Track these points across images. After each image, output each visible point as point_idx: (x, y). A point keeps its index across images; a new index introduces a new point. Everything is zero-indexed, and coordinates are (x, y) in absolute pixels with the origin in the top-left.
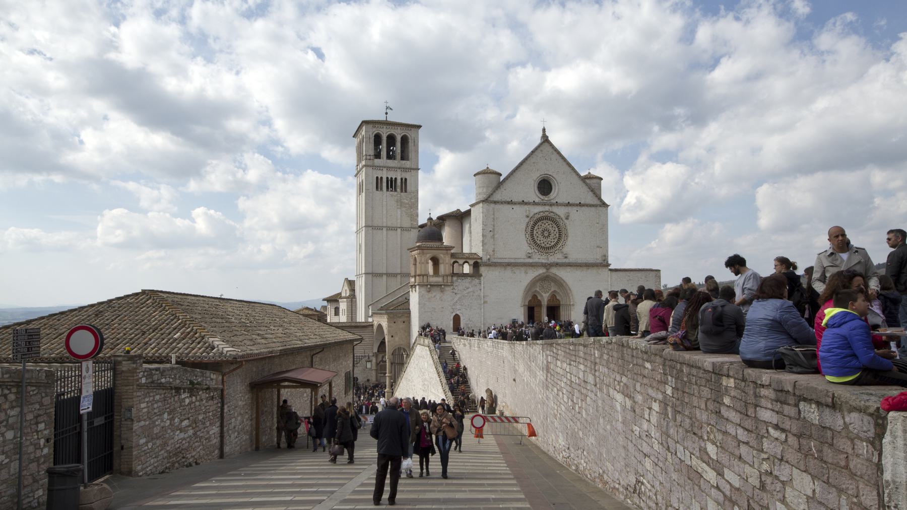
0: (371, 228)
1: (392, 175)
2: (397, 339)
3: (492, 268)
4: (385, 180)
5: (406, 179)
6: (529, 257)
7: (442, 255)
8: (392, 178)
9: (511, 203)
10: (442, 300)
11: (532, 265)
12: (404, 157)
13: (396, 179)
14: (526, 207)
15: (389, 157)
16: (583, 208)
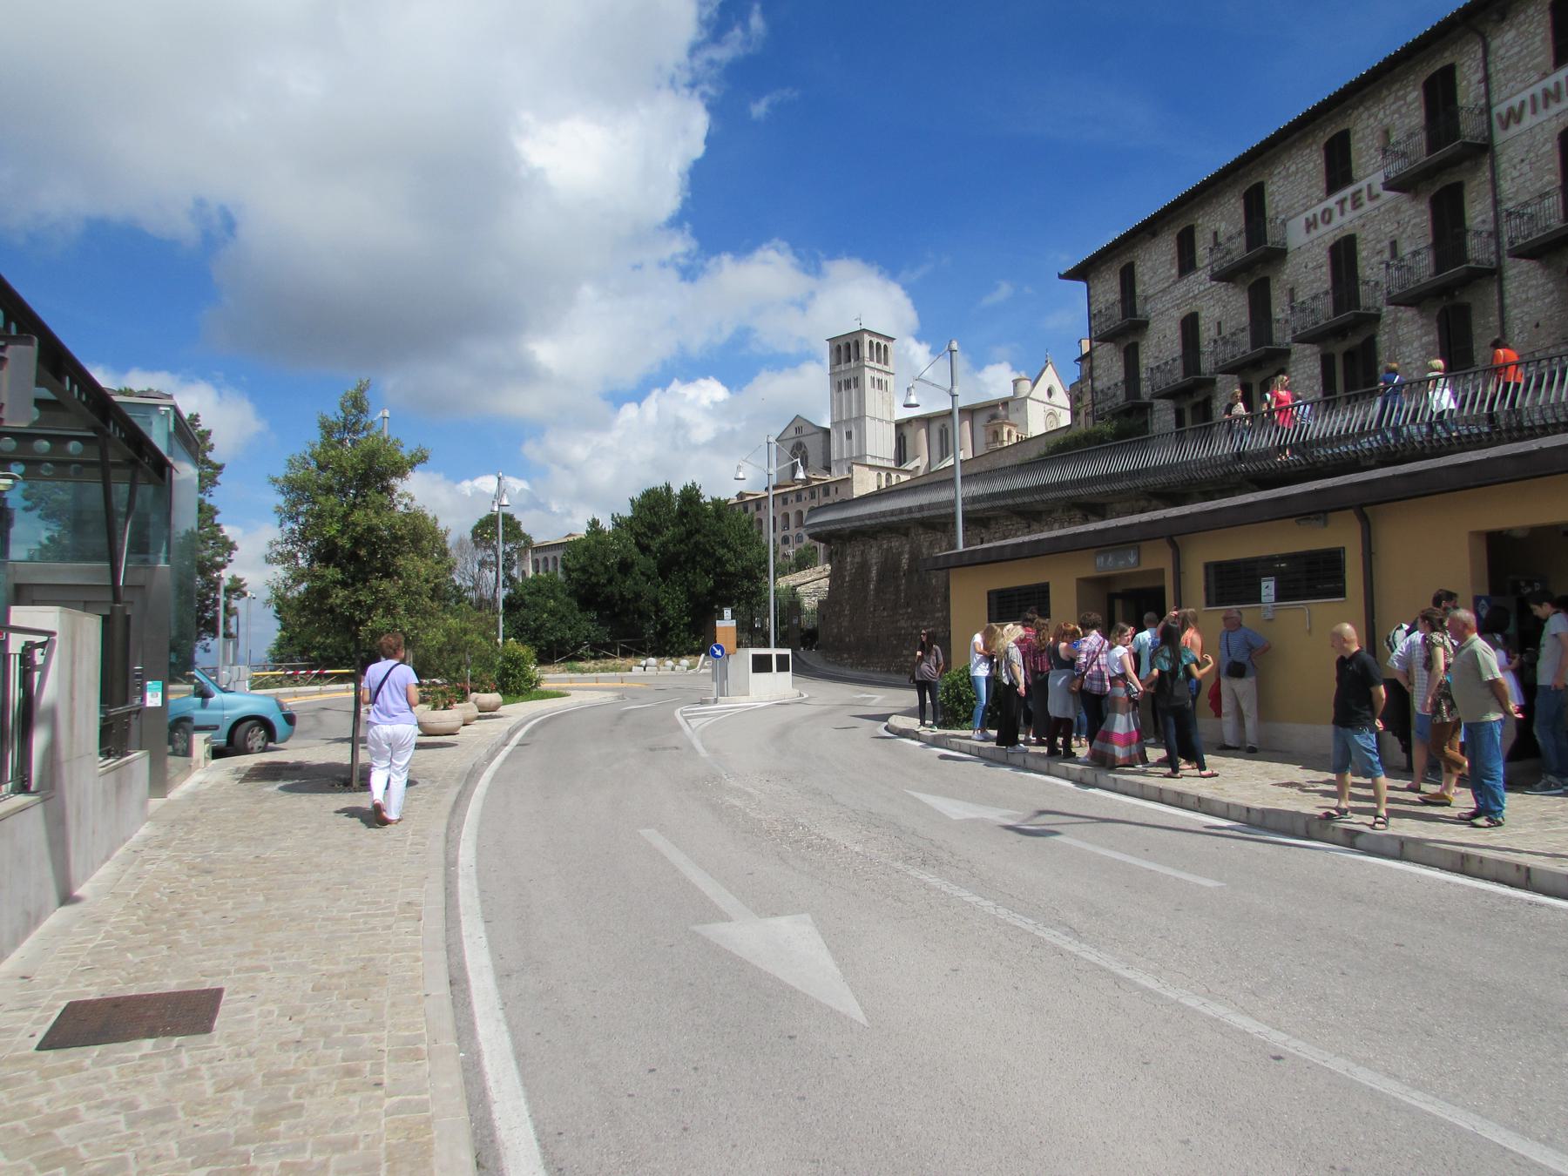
12: (886, 363)
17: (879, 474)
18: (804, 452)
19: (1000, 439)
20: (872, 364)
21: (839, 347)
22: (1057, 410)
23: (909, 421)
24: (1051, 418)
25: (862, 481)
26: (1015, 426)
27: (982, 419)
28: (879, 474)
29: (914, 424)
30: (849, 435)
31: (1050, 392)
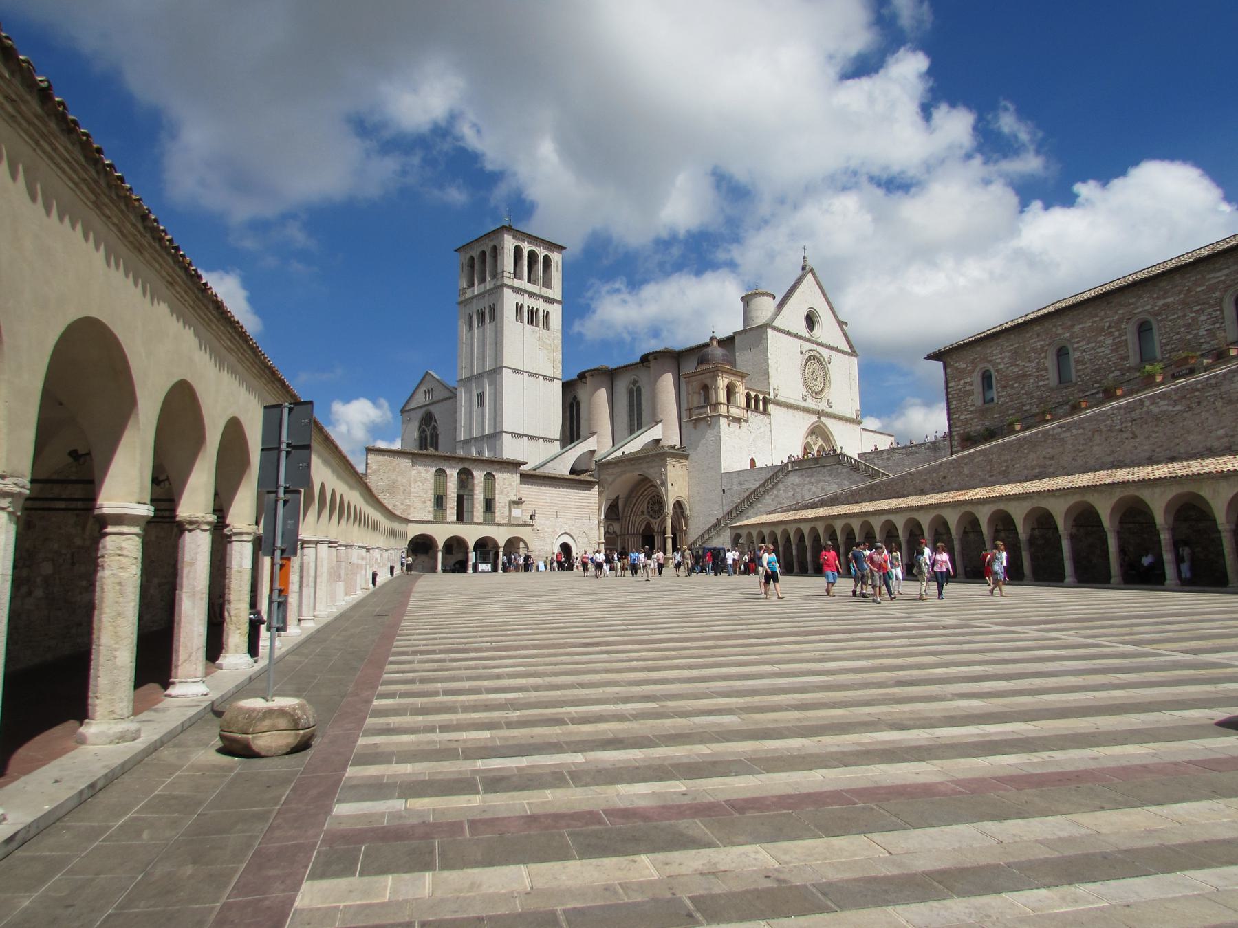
1: (534, 303)
2: (676, 489)
3: (778, 407)
5: (548, 313)
8: (533, 308)
9: (788, 333)
10: (740, 438)
11: (808, 411)
14: (800, 341)
15: (529, 281)
16: (840, 354)
17: (441, 473)
18: (435, 428)
20: (517, 283)
21: (472, 258)
22: (825, 353)
23: (582, 376)
24: (813, 365)
25: (392, 489)
26: (743, 376)
27: (690, 367)
28: (441, 473)
29: (589, 380)
30: (481, 397)
31: (811, 321)
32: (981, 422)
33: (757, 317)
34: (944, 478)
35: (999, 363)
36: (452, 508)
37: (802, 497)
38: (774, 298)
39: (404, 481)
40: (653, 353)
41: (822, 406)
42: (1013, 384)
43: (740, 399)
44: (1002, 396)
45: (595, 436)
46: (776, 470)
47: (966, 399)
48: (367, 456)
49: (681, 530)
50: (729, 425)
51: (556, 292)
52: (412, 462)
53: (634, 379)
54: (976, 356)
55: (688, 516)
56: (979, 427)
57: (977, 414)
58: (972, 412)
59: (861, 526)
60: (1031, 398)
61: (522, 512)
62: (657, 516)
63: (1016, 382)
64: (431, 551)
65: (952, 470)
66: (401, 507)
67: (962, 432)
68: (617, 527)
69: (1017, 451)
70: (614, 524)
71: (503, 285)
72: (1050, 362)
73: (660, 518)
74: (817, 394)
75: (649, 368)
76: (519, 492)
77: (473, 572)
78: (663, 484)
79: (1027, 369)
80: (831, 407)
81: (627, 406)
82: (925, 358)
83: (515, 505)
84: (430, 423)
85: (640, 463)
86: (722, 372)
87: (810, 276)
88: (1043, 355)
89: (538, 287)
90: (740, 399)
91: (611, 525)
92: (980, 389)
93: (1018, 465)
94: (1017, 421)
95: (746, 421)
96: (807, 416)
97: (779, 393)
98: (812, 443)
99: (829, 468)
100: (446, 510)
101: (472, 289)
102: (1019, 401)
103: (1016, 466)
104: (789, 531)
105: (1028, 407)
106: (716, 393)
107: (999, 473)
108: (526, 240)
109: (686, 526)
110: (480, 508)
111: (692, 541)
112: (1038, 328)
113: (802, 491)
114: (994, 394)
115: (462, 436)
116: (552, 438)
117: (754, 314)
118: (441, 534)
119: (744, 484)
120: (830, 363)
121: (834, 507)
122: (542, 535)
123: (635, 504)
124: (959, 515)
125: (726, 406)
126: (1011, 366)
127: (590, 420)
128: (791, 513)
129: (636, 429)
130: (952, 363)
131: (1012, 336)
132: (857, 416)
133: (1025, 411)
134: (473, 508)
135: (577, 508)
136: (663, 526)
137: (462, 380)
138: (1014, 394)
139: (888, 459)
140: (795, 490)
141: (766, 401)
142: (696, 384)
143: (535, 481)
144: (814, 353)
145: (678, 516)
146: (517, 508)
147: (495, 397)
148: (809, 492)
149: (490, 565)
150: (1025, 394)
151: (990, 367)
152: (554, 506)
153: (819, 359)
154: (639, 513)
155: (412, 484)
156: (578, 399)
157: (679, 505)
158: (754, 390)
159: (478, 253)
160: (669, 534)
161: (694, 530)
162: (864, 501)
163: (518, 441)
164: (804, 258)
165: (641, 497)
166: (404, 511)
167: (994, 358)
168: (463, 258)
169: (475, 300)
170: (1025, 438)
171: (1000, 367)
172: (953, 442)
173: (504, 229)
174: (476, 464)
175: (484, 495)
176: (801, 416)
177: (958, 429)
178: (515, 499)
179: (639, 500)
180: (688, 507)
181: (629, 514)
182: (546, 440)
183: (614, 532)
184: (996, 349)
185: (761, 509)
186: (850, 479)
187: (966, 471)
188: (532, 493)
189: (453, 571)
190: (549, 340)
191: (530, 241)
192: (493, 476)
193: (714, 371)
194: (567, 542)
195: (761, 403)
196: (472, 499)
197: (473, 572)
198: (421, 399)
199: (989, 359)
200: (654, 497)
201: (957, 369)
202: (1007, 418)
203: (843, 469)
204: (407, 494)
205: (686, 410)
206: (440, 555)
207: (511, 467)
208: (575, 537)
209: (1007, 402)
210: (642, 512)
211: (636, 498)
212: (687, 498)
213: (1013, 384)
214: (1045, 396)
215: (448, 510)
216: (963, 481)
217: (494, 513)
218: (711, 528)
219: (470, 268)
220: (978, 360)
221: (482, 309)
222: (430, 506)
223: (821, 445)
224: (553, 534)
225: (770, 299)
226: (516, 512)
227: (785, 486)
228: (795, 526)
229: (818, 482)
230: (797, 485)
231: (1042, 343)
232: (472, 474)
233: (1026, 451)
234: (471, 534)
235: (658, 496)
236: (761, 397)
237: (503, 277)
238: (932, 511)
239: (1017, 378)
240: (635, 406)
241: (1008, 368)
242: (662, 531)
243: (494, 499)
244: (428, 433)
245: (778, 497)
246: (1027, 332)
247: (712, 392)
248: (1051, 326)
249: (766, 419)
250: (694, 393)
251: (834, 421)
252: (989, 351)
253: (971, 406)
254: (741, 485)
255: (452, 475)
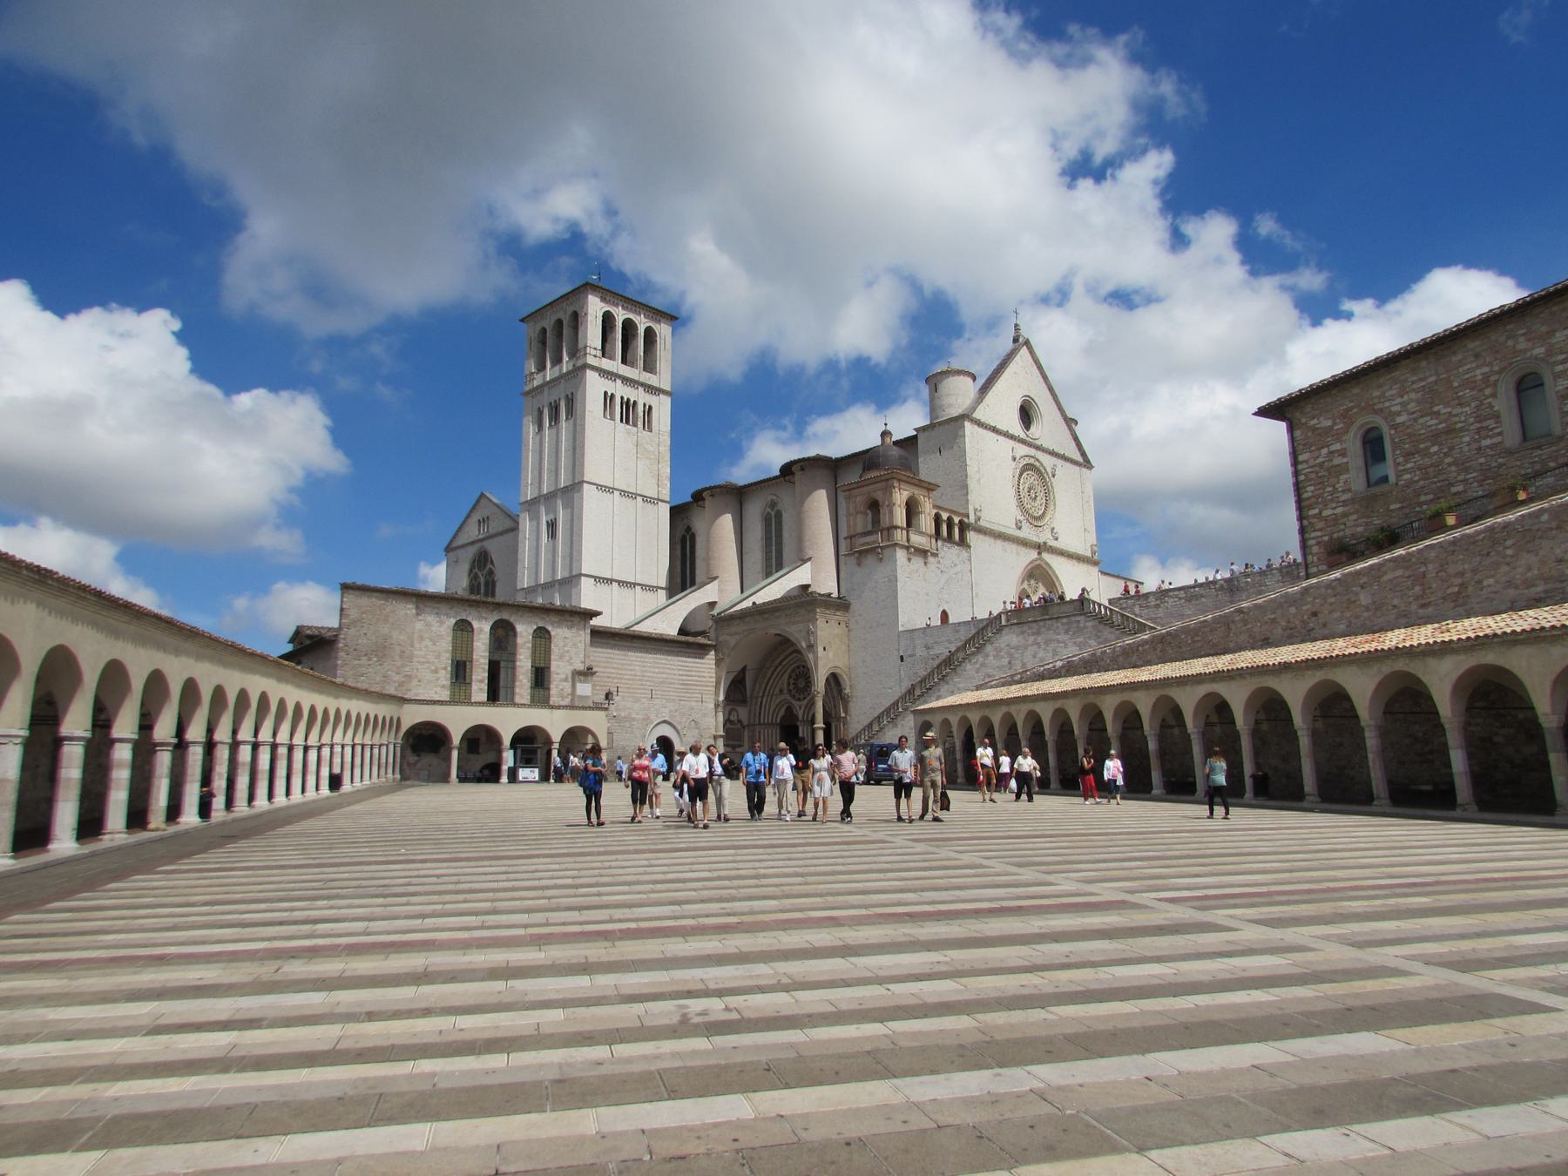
0: (595, 487)
2: (831, 655)
4: (618, 401)
5: (650, 407)
6: (1020, 528)
7: (922, 497)
8: (628, 400)
9: (994, 430)
10: (925, 580)
13: (635, 402)
14: (1011, 443)
15: (622, 362)
16: (1068, 465)
17: (463, 627)
18: (491, 573)
19: (885, 521)
20: (606, 364)
21: (544, 331)
22: (1047, 461)
23: (698, 497)
24: (1030, 479)
25: (381, 651)
26: (930, 488)
27: (852, 476)
28: (463, 627)
29: (708, 502)
30: (552, 526)
32: (1365, 520)
33: (950, 406)
34: (1315, 614)
35: (1399, 414)
36: (482, 681)
37: (1024, 665)
38: (974, 379)
39: (402, 637)
40: (799, 461)
41: (1044, 537)
42: (1427, 448)
43: (926, 522)
44: (1406, 471)
45: (716, 582)
46: (981, 626)
47: (1333, 481)
48: (342, 597)
49: (839, 718)
50: (909, 560)
51: (663, 379)
52: (417, 608)
53: (772, 500)
54: (1352, 404)
55: (849, 697)
56: (1360, 529)
57: (1357, 506)
58: (1345, 503)
59: (1155, 705)
60: (1467, 470)
61: (593, 689)
62: (802, 697)
63: (1433, 445)
64: (442, 749)
65: (1332, 600)
66: (396, 678)
67: (1326, 538)
68: (743, 713)
69: (1488, 554)
70: (737, 708)
71: (586, 366)
72: (1504, 403)
73: (806, 701)
74: (1036, 520)
75: (794, 483)
76: (589, 657)
77: (509, 782)
78: (811, 647)
79: (1457, 419)
80: (1057, 539)
81: (762, 539)
82: (1253, 414)
83: (582, 678)
84: (485, 565)
85: (777, 618)
86: (899, 480)
87: (1024, 351)
88: (1488, 391)
89: (637, 371)
90: (926, 522)
91: (737, 712)
92: (1360, 462)
93: (1491, 581)
94: (1450, 510)
95: (935, 555)
96: (1022, 550)
97: (983, 515)
98: (1029, 591)
99: (1065, 620)
100: (470, 684)
101: (541, 374)
102: (1441, 477)
103: (1485, 583)
104: (1015, 715)
105: (1460, 488)
106: (891, 512)
107: (1444, 598)
108: (620, 303)
109: (846, 711)
110: (525, 681)
111: (854, 734)
112: (1478, 343)
113: (1022, 656)
114: (1388, 468)
115: (525, 581)
116: (655, 585)
117: (946, 401)
118: (458, 721)
119: (933, 648)
120: (1054, 476)
121: (1093, 675)
122: (627, 724)
123: (769, 679)
124: (1377, 680)
125: (905, 532)
126: (1422, 417)
127: (708, 559)
128: (1014, 687)
129: (774, 571)
130: (1303, 421)
131: (1424, 364)
132: (1093, 553)
133: (1455, 494)
134: (514, 681)
135: (682, 684)
136: (811, 714)
137: (527, 502)
138: (1432, 465)
139: (1157, 606)
140: (1011, 656)
141: (964, 527)
142: (860, 499)
143: (618, 643)
144: (1032, 461)
145: (833, 697)
146: (585, 682)
147: (572, 525)
148: (1034, 657)
149: (537, 770)
150: (1455, 463)
151: (1378, 421)
152: (646, 681)
153: (1039, 470)
154: (777, 691)
155: (415, 642)
156: (693, 530)
157: (834, 680)
158: (946, 510)
159: (552, 322)
160: (820, 724)
161: (858, 716)
162: (1149, 663)
163: (604, 588)
164: (1016, 325)
165: (780, 668)
166: (400, 686)
167: (1387, 404)
168: (530, 331)
169: (546, 389)
170: (1506, 526)
171: (1399, 420)
172: (1310, 558)
173: (588, 288)
174: (520, 613)
175: (533, 662)
176: (1015, 551)
177: (1319, 534)
178: (582, 668)
179: (778, 670)
180: (848, 683)
181: (761, 695)
182: (645, 587)
183: (739, 721)
184: (1391, 389)
185: (960, 685)
186: (1099, 637)
187: (1364, 599)
188: (611, 661)
189: (479, 780)
190: (652, 446)
191: (625, 305)
192: (548, 632)
193: (887, 480)
194: (666, 734)
195: (956, 530)
196: (514, 668)
197: (509, 782)
198: (472, 532)
199: (1377, 407)
200: (798, 667)
201: (1314, 429)
202: (1417, 509)
203: (1086, 621)
204: (407, 657)
205: (845, 538)
206: (455, 754)
207: (576, 619)
208: (679, 728)
209: (1418, 481)
210: (781, 691)
211: (772, 669)
212: (846, 670)
213: (1427, 448)
214: (1495, 464)
215: (473, 683)
216: (1357, 617)
217: (549, 689)
218: (883, 713)
219: (540, 345)
220: (1355, 410)
221: (555, 401)
222: (445, 677)
223: (1043, 594)
224: (645, 723)
225: (969, 380)
226: (584, 689)
227: (996, 649)
228: (1025, 708)
229: (1048, 642)
230: (1017, 648)
231: (1486, 369)
232: (513, 629)
233: (1509, 552)
234: (507, 721)
235: (804, 667)
236: (956, 520)
237: (585, 354)
238: (1310, 673)
239: (1435, 437)
240: (774, 538)
241: (1415, 420)
242: (810, 719)
243: (549, 668)
244: (482, 580)
245: (986, 666)
246: (1455, 353)
247: (884, 511)
248: (1502, 339)
249: (964, 554)
250: (857, 513)
251: (1062, 560)
252: (1376, 393)
253: (1343, 491)
254: (928, 648)
255: (481, 630)
